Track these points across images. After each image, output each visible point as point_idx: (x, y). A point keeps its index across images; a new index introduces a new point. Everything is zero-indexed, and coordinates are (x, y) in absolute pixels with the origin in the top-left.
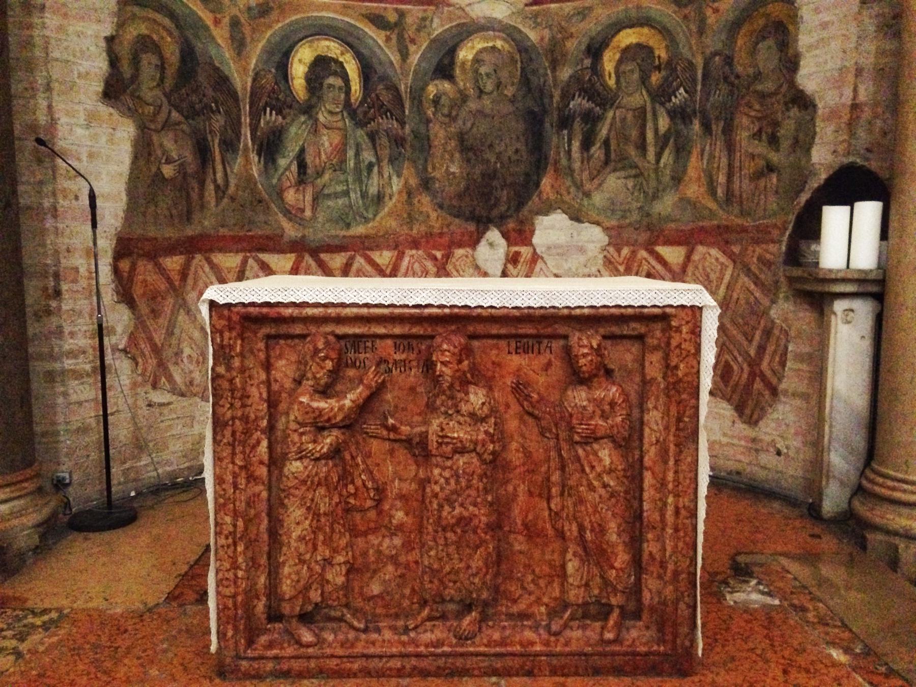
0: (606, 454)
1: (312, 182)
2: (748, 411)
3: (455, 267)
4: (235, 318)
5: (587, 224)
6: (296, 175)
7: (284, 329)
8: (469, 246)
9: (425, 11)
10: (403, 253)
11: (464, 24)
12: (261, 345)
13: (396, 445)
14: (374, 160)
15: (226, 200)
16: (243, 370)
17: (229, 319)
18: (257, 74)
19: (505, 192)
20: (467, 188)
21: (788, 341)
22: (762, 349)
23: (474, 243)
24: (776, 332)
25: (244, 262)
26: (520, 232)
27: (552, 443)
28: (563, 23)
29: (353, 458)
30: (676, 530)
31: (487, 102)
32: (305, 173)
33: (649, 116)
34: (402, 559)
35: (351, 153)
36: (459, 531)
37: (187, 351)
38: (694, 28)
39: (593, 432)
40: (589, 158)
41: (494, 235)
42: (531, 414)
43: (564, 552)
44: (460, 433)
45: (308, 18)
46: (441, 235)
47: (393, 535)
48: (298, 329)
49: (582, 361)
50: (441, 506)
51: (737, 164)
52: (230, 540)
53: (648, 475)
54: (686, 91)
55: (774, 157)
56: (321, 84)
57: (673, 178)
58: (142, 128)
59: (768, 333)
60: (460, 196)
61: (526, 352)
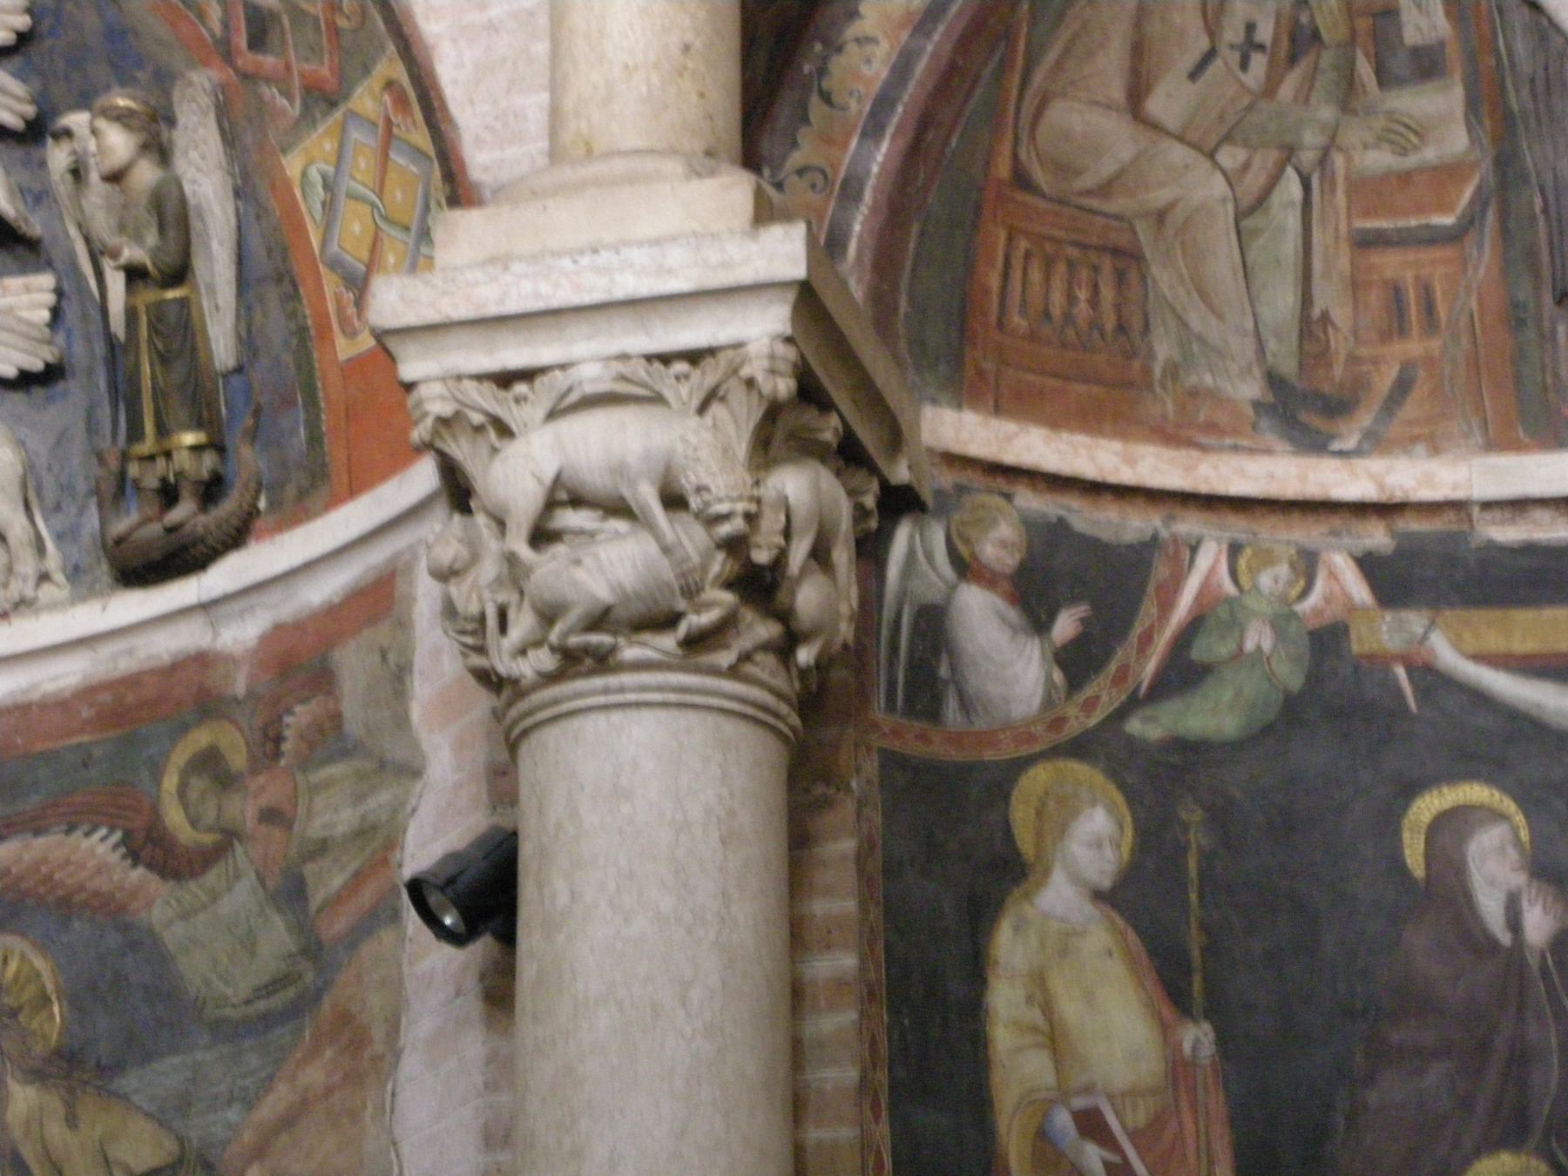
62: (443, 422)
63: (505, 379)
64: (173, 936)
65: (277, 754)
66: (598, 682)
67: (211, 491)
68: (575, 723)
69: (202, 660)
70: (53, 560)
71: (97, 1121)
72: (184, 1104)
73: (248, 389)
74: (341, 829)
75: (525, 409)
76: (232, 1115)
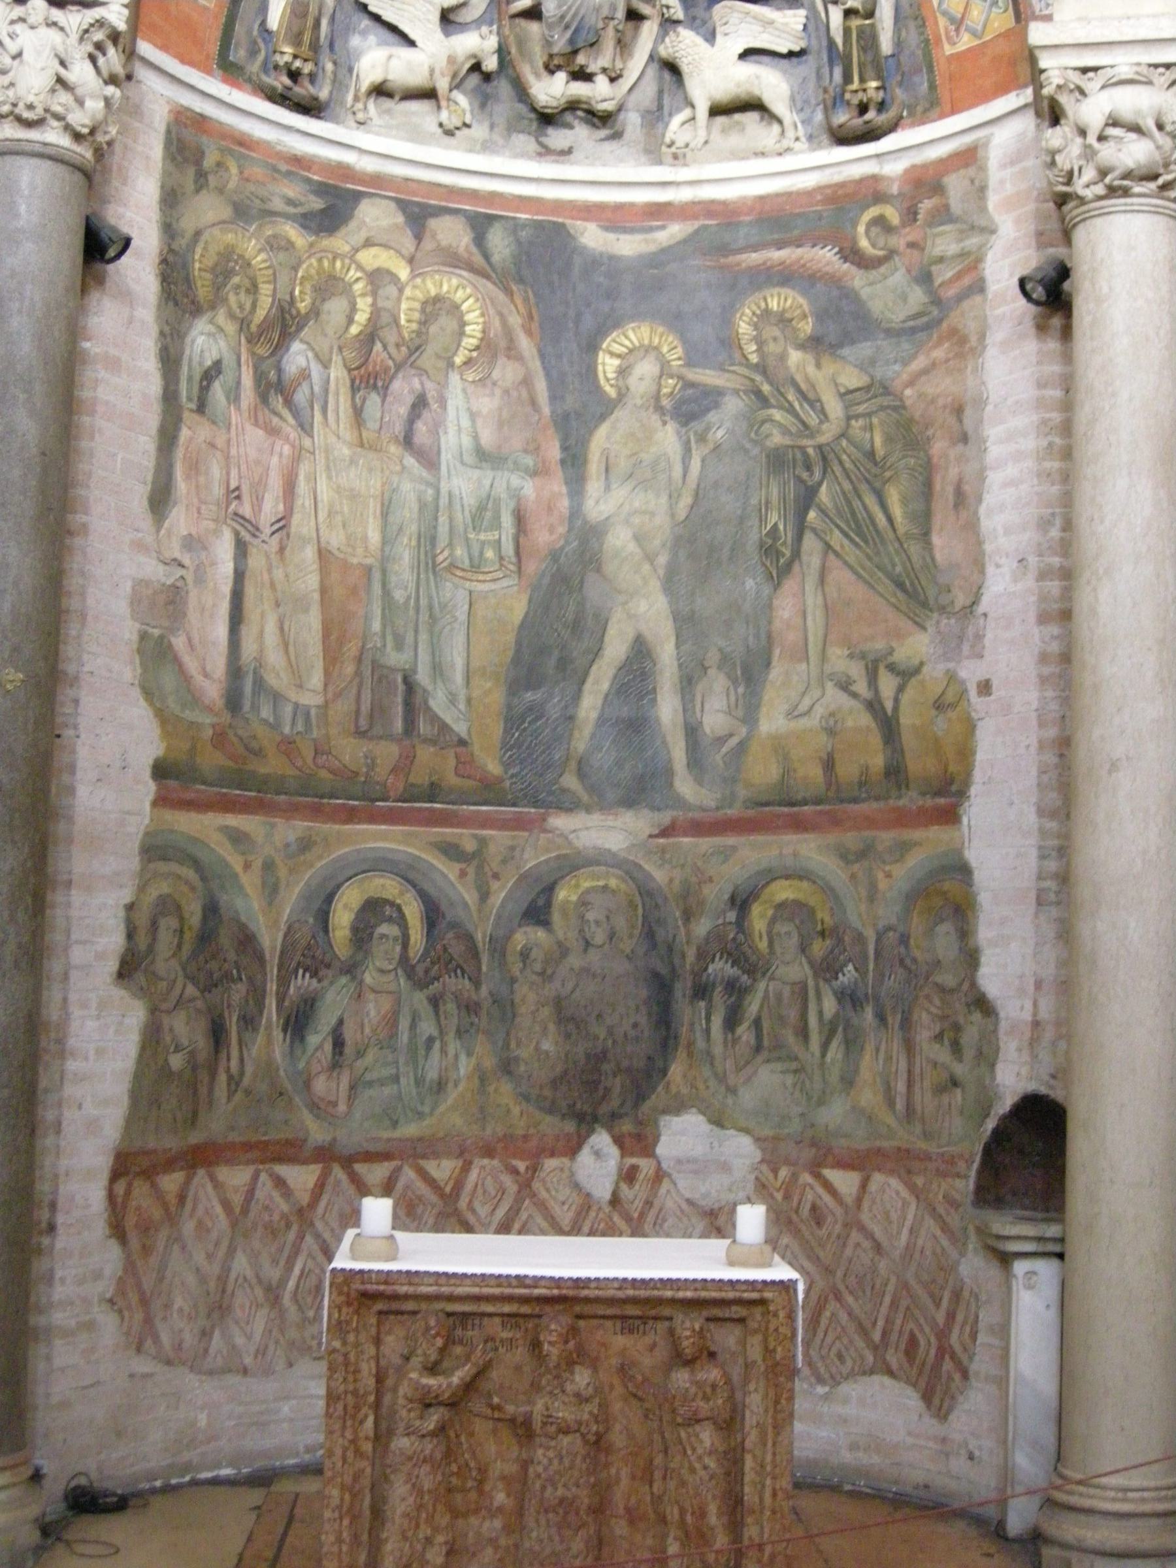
0: (707, 1436)
1: (351, 1066)
2: (936, 1401)
3: (543, 1181)
4: (353, 1294)
5: (732, 1132)
6: (329, 1056)
7: (395, 1306)
8: (563, 1154)
9: (514, 837)
10: (471, 1163)
11: (565, 856)
12: (373, 1321)
13: (500, 1425)
14: (436, 1033)
15: (239, 1096)
16: (357, 1345)
17: (348, 1295)
18: (289, 928)
19: (618, 1080)
20: (566, 1072)
21: (978, 1307)
22: (951, 1316)
23: (573, 1150)
24: (966, 1294)
25: (256, 1177)
26: (639, 1137)
27: (655, 1425)
28: (699, 864)
29: (457, 1436)
30: (774, 1512)
31: (594, 956)
32: (341, 1053)
33: (811, 993)
34: (503, 1542)
35: (404, 1024)
36: (561, 1511)
37: (179, 1302)
38: (864, 893)
39: (695, 1413)
40: (735, 1041)
41: (601, 1139)
42: (635, 1396)
43: (664, 1537)
44: (564, 1413)
45: (358, 851)
46: (526, 1137)
47: (493, 1516)
48: (410, 1306)
49: (685, 1343)
50: (544, 1488)
51: (917, 1071)
52: (336, 1515)
53: (748, 1458)
54: (856, 969)
55: (959, 1070)
56: (371, 934)
57: (842, 1078)
58: (153, 1011)
59: (957, 1296)
60: (555, 1083)
61: (631, 1331)
62: (1059, 87)
63: (1085, 70)
64: (865, 293)
65: (915, 220)
66: (1122, 201)
67: (882, 106)
68: (1111, 217)
69: (875, 178)
70: (801, 132)
71: (829, 367)
72: (873, 362)
73: (899, 64)
74: (949, 253)
75: (1092, 84)
76: (897, 367)
